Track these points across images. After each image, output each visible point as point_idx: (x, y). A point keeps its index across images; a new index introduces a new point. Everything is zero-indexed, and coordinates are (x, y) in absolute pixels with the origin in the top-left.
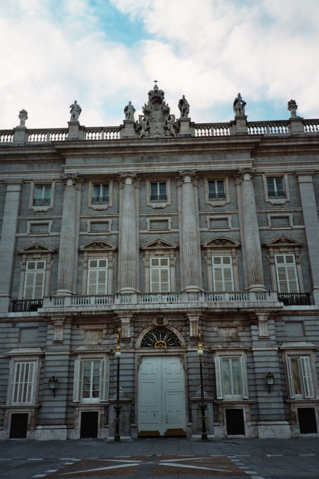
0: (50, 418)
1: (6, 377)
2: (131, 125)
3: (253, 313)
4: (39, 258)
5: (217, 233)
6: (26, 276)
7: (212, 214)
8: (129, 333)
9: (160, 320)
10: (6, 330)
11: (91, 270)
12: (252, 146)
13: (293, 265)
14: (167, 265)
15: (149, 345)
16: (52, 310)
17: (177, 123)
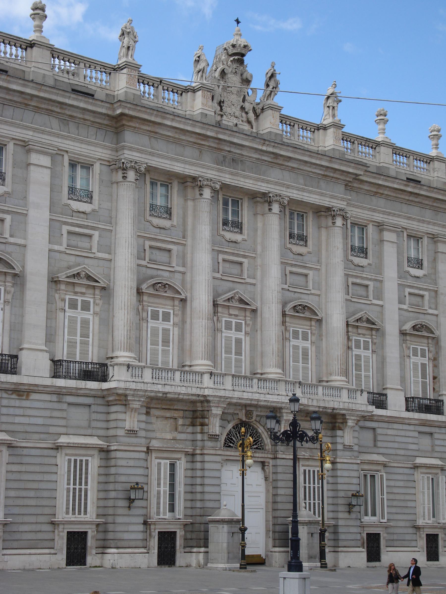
0: (125, 538)
1: (53, 477)
2: (209, 93)
3: (344, 415)
4: (83, 294)
5: (296, 294)
6: (67, 320)
7: (292, 265)
8: (218, 428)
9: (249, 414)
10: (50, 405)
11: (152, 323)
12: (350, 177)
13: (369, 353)
14: (242, 332)
15: (232, 445)
16: (133, 386)
17: (260, 106)
